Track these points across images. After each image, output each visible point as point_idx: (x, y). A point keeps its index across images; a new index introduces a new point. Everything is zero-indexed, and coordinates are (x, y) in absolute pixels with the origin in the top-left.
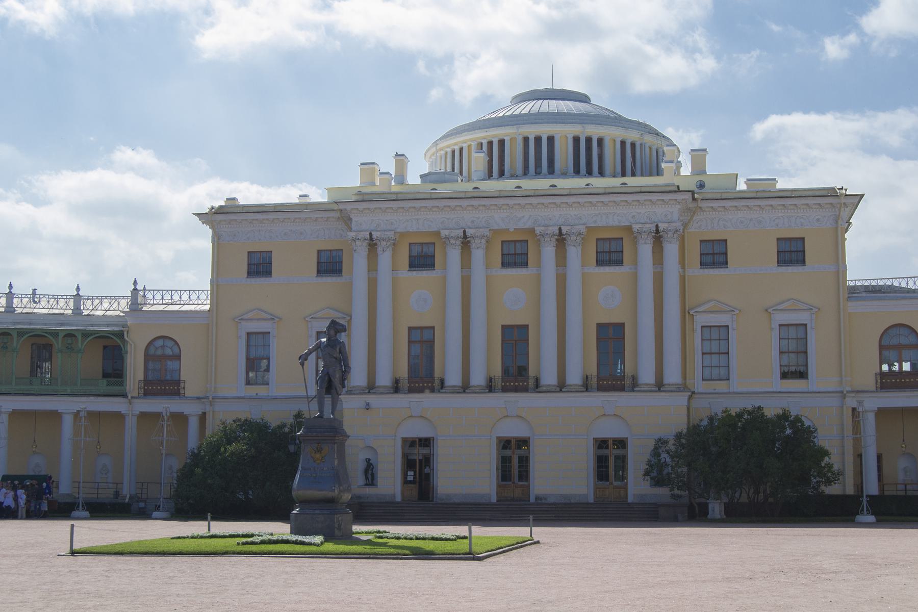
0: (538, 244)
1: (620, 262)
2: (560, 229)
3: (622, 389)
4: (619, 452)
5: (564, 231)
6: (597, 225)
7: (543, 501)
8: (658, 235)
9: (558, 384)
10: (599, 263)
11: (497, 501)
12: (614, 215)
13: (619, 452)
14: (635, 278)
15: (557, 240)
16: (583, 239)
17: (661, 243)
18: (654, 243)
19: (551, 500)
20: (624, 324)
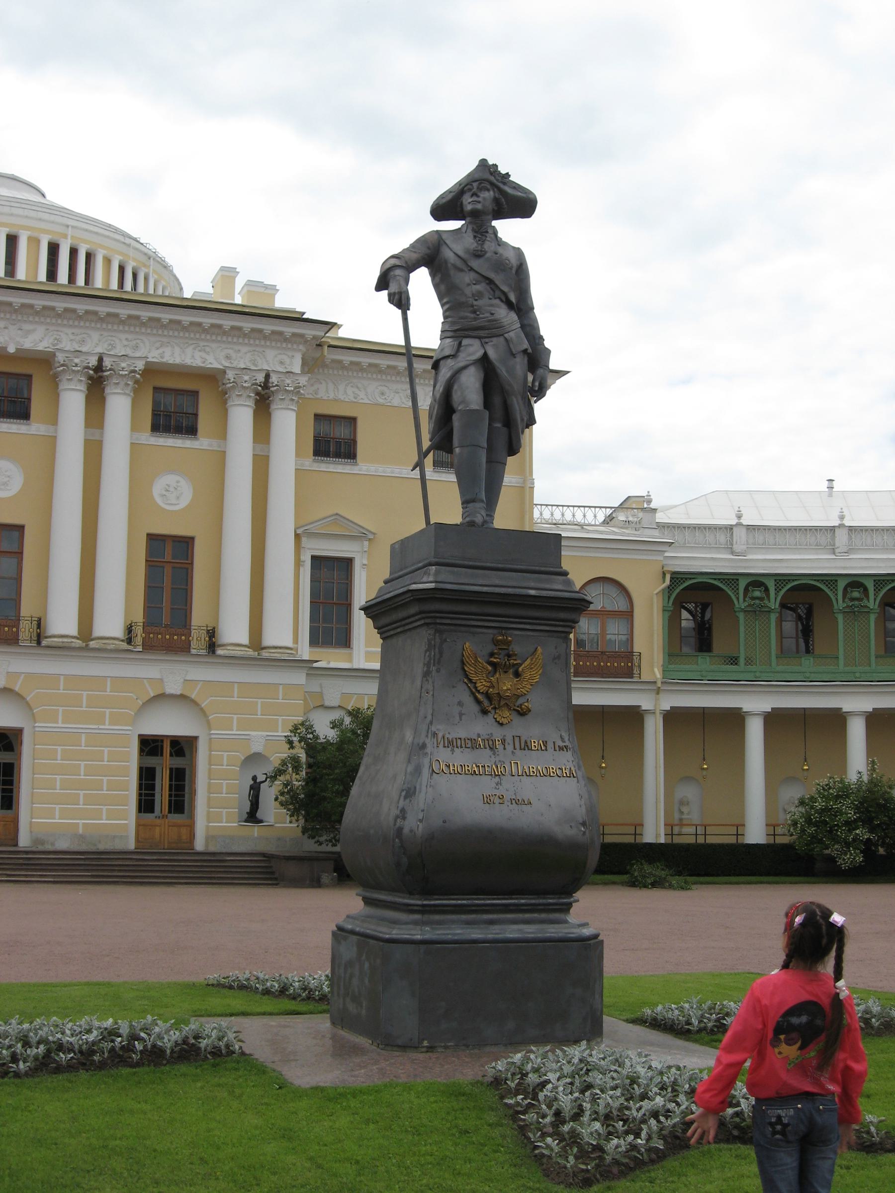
0: (54, 381)
1: (191, 431)
2: (100, 360)
3: (184, 648)
4: (178, 762)
5: (107, 363)
6: (164, 360)
7: (49, 847)
8: (263, 393)
9: (79, 633)
10: (156, 428)
11: (135, 849)
12: (194, 349)
13: (178, 762)
14: (221, 459)
15: (90, 378)
16: (137, 382)
17: (268, 406)
18: (257, 402)
19: (63, 845)
20: (192, 539)
